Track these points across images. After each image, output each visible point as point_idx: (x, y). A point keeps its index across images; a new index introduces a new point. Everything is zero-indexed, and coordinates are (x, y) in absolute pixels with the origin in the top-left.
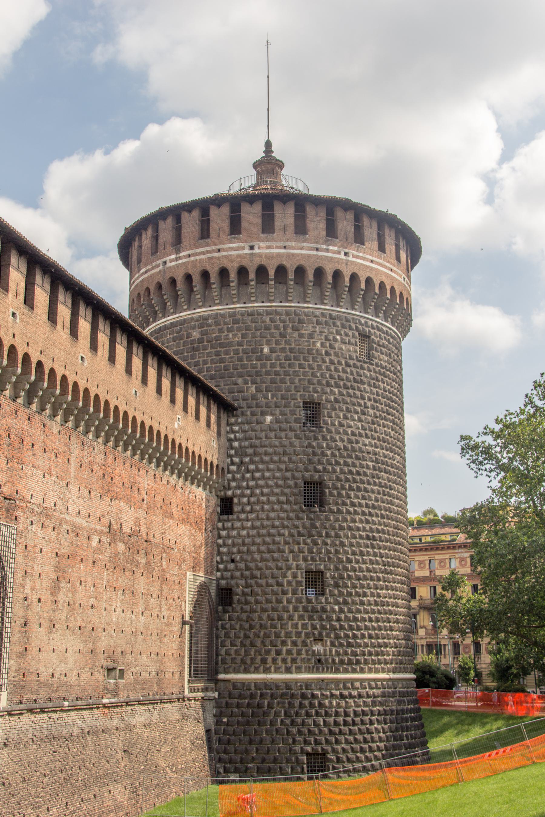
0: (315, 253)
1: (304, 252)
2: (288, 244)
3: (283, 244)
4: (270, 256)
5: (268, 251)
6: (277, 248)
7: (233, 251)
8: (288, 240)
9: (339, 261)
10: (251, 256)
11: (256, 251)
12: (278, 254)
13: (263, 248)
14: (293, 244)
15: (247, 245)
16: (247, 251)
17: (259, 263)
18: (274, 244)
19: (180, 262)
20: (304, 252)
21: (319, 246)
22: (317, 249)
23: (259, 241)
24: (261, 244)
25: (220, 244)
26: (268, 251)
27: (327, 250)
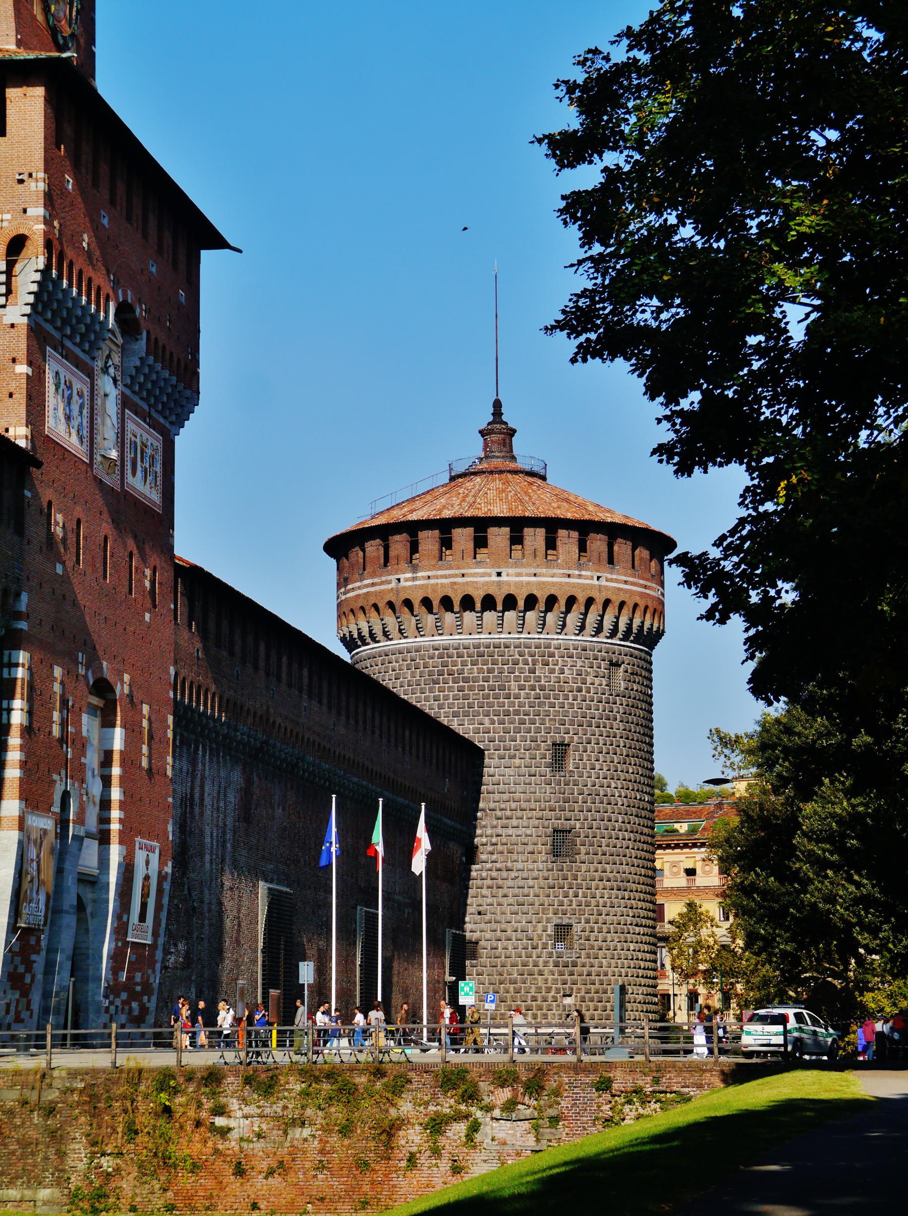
0: (567, 580)
1: (555, 580)
2: (538, 571)
3: (533, 571)
4: (519, 585)
5: (517, 579)
6: (528, 575)
7: (479, 576)
8: (538, 566)
9: (592, 587)
10: (499, 584)
11: (504, 578)
12: (528, 583)
13: (512, 575)
14: (544, 571)
15: (494, 572)
16: (495, 578)
17: (507, 593)
18: (524, 571)
19: (417, 583)
20: (555, 580)
21: (570, 572)
22: (569, 576)
23: (507, 567)
24: (511, 571)
25: (464, 568)
26: (517, 579)
27: (580, 576)
